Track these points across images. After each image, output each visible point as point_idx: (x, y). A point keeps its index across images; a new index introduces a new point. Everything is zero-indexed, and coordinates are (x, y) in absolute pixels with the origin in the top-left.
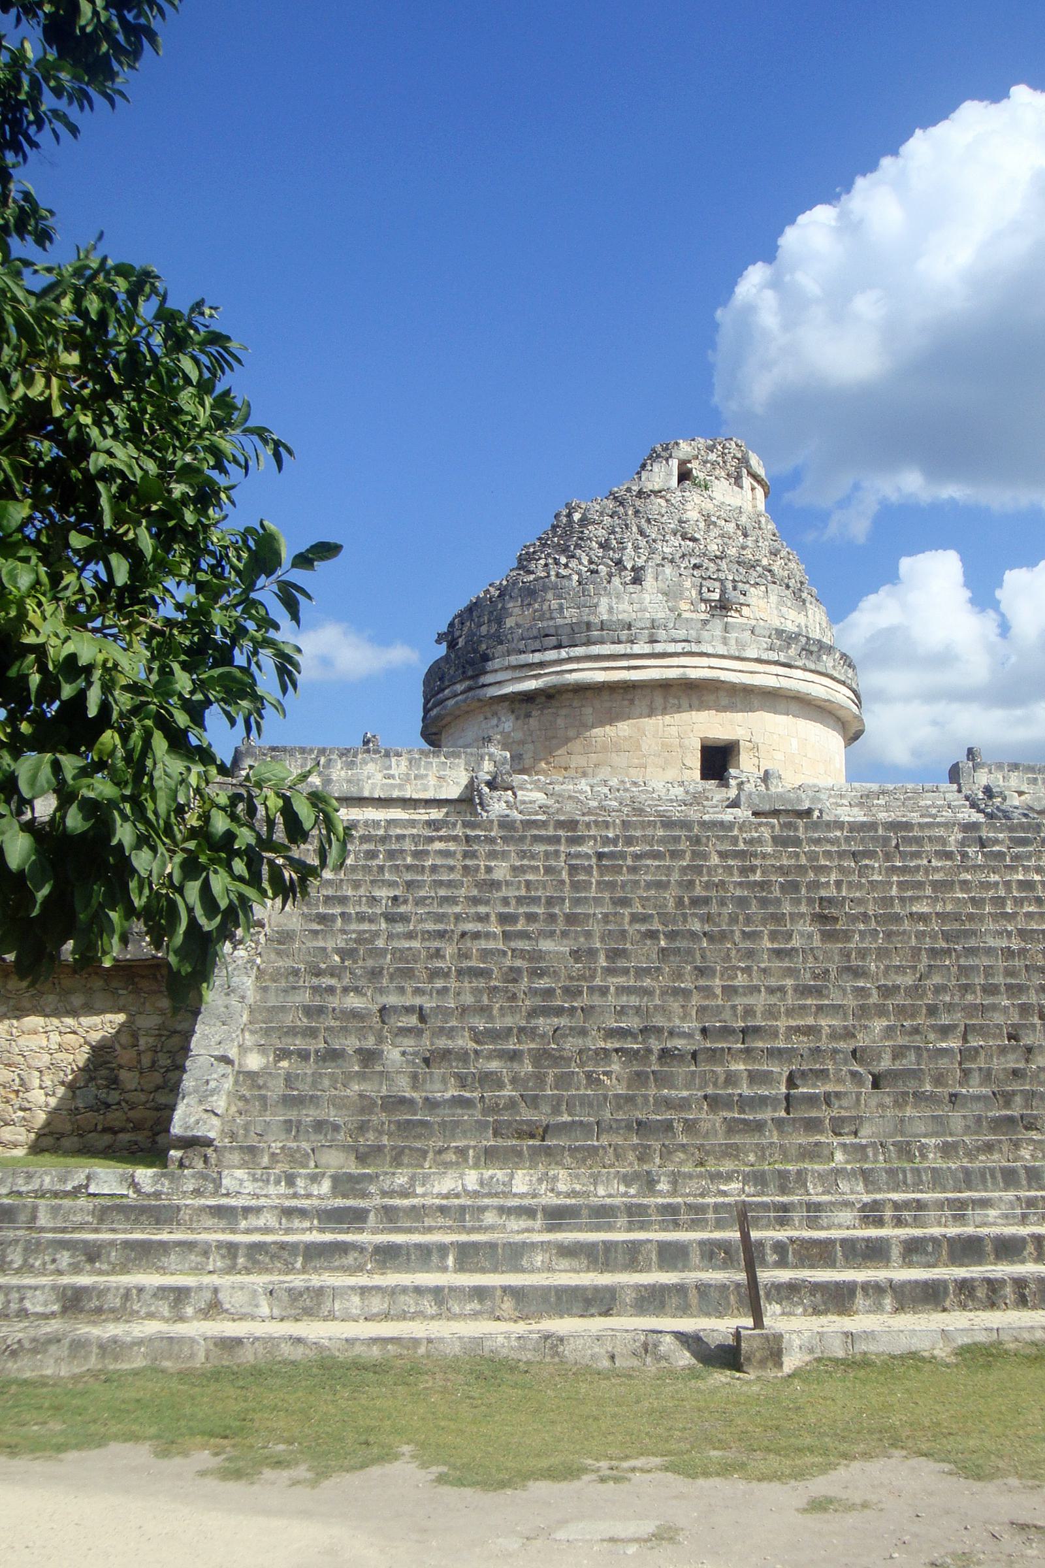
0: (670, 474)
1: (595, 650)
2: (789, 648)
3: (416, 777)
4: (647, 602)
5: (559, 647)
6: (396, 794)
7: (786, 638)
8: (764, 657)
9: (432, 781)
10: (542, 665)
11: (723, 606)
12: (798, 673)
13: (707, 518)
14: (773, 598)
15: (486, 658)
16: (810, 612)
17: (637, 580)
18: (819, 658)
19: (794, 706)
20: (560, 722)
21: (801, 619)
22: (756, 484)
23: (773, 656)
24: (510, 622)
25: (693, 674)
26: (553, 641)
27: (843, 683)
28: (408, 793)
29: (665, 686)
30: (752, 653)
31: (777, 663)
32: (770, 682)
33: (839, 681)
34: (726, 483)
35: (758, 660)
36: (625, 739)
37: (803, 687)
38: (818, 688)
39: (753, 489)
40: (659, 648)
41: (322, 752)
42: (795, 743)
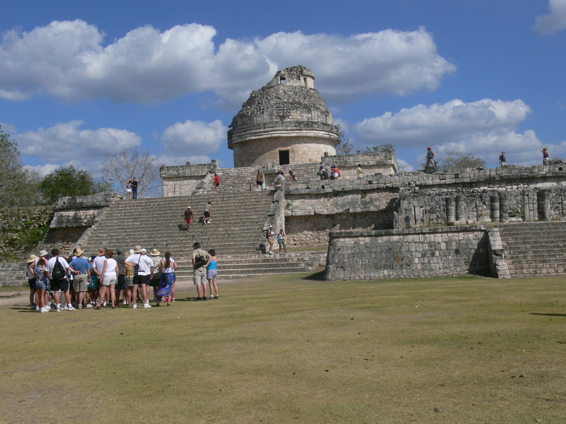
0: (278, 80)
1: (252, 131)
2: (300, 125)
4: (266, 117)
5: (245, 131)
7: (299, 124)
9: (200, 171)
10: (242, 135)
11: (283, 117)
12: (304, 131)
13: (285, 92)
14: (299, 112)
15: (233, 134)
17: (263, 113)
18: (312, 126)
19: (305, 140)
21: (309, 115)
24: (238, 124)
25: (274, 135)
26: (243, 130)
27: (322, 131)
28: (196, 174)
29: (270, 138)
30: (289, 128)
31: (297, 130)
32: (295, 135)
34: (295, 79)
35: (291, 130)
37: (305, 135)
38: (311, 133)
39: (305, 79)
40: (266, 130)
41: (177, 167)
42: (306, 148)
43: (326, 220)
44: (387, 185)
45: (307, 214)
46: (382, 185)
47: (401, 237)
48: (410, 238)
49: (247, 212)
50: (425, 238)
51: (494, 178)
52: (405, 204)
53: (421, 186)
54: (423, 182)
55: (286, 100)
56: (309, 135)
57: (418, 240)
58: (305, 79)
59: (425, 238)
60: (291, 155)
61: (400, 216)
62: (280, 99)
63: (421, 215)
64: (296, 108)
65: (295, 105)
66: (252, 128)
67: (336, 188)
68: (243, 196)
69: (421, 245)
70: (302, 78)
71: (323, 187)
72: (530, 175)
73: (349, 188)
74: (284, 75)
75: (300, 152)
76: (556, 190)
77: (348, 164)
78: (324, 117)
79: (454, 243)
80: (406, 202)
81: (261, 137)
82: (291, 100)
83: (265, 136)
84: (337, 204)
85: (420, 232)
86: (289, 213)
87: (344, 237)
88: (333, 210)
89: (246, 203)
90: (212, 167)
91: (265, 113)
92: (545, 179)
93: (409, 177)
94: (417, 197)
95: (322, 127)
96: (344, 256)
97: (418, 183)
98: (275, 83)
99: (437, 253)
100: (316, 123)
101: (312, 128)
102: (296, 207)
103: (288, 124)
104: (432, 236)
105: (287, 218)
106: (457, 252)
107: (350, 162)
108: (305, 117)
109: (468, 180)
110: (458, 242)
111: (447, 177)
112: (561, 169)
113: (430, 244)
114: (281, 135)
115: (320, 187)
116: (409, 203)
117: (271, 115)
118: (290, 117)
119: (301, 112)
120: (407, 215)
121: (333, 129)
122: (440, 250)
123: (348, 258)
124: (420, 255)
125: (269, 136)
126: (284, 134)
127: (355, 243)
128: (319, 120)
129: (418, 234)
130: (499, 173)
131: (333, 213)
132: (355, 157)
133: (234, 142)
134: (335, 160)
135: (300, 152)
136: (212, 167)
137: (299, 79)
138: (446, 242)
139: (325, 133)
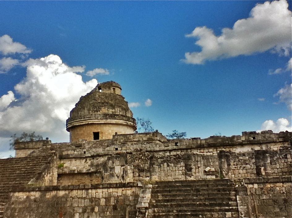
1: (77, 120)
3: (37, 145)
6: (34, 147)
8: (101, 118)
10: (72, 123)
12: (109, 120)
13: (99, 96)
14: (106, 108)
16: (116, 109)
19: (110, 125)
20: (75, 131)
21: (114, 110)
22: (114, 88)
23: (103, 118)
25: (90, 123)
29: (88, 124)
32: (103, 122)
33: (120, 120)
34: (107, 89)
35: (100, 119)
36: (83, 133)
37: (109, 122)
38: (114, 121)
39: (114, 89)
42: (110, 131)
43: (86, 176)
44: (128, 151)
45: (72, 172)
46: (124, 151)
47: (67, 192)
48: (74, 193)
49: (27, 171)
50: (87, 194)
51: (203, 145)
52: (110, 164)
53: (150, 151)
54: (152, 149)
55: (99, 101)
56: (112, 122)
57: (81, 196)
58: (114, 89)
59: (87, 194)
60: (100, 135)
61: (105, 174)
62: (96, 100)
63: (122, 173)
64: (105, 106)
65: (104, 104)
66: (77, 118)
67: (92, 154)
68: (30, 159)
69: (83, 201)
70: (112, 88)
71: (85, 152)
72: (230, 143)
73: (102, 153)
74: (101, 86)
75: (106, 133)
76: (249, 154)
77: (129, 140)
78: (124, 112)
79: (112, 200)
80: (111, 162)
81: (82, 124)
82: (103, 101)
83: (84, 123)
84: (93, 165)
85: (83, 187)
86: (61, 171)
87: (19, 192)
88: (90, 169)
89: (30, 164)
90: (45, 142)
91: (86, 109)
92: (242, 145)
93: (143, 145)
94: (119, 157)
95: (122, 117)
96: (15, 210)
97: (149, 149)
98: (94, 91)
99: (96, 209)
100: (117, 115)
101: (114, 118)
102: (66, 167)
103: (99, 116)
104: (94, 191)
105: (60, 176)
106: (115, 208)
107: (131, 139)
108: (111, 111)
109: (184, 147)
110: (117, 199)
111: (170, 145)
112: (254, 138)
113: (91, 200)
114: (94, 122)
115: (83, 152)
116: (113, 163)
117: (89, 110)
118: (101, 111)
119: (108, 108)
120: (111, 172)
121: (130, 119)
122: (99, 205)
123: (19, 212)
124: (81, 211)
125: (87, 123)
126: (96, 121)
127: (28, 197)
128: (121, 113)
129: (82, 189)
130: (207, 141)
131: (90, 171)
132: (134, 135)
133: (68, 127)
134: (121, 137)
135: (106, 133)
136: (45, 142)
137: (110, 89)
138: (105, 198)
139: (124, 121)
